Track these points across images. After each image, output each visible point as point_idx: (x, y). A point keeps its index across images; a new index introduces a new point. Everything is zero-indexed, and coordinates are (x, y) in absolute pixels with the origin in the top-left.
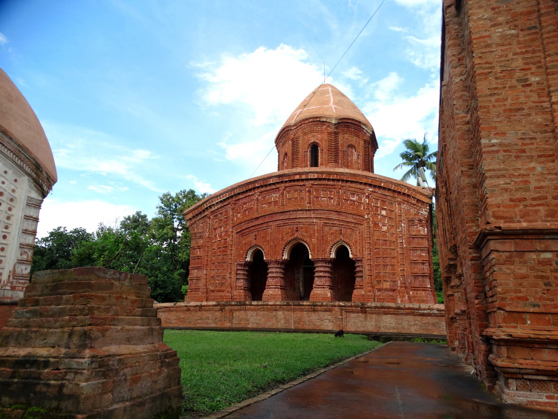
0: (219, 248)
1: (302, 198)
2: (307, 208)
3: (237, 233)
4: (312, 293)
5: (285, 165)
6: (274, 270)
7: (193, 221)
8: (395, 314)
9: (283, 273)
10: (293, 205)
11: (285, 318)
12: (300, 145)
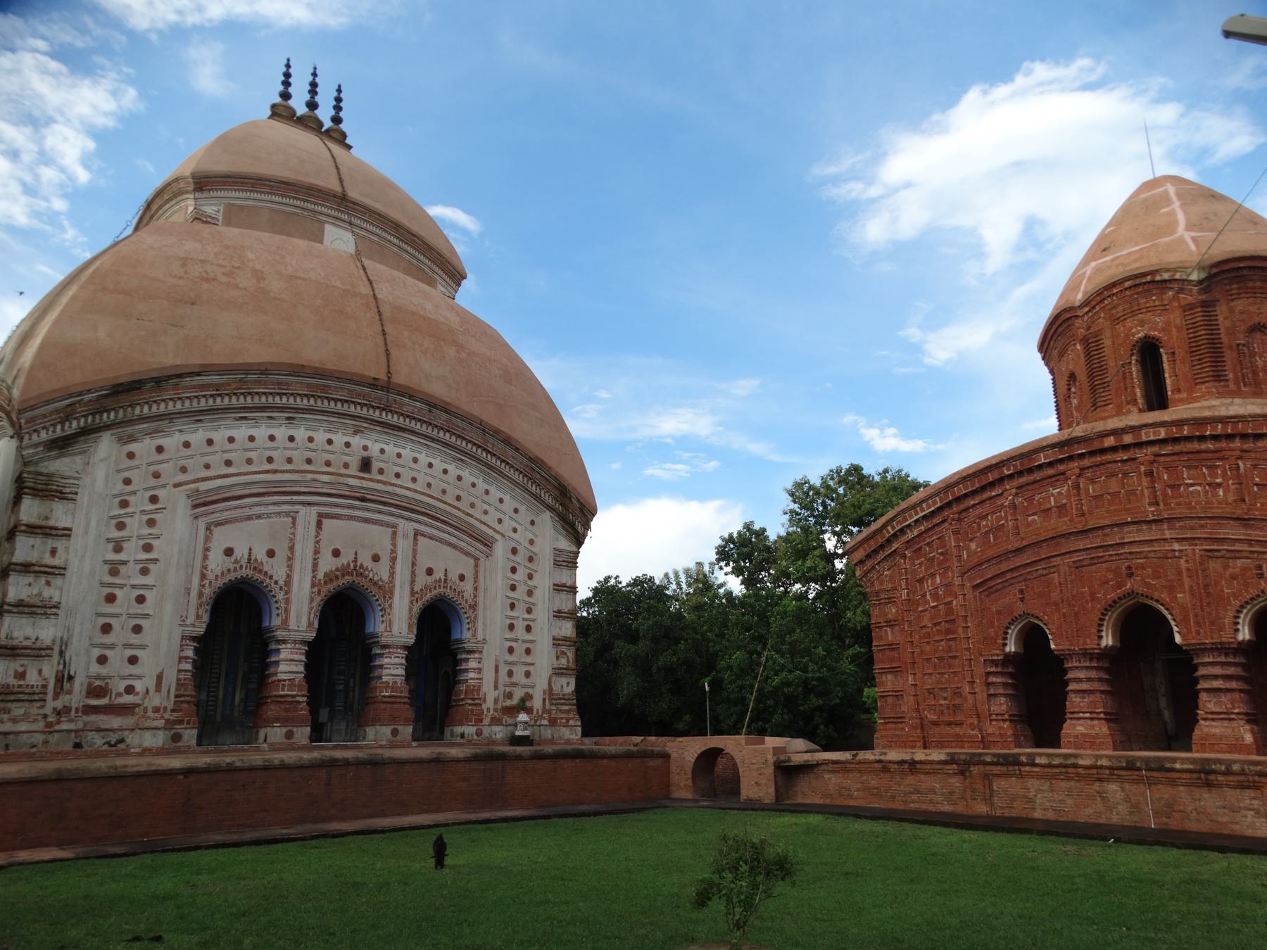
0: (935, 625)
1: (1132, 492)
2: (1151, 517)
3: (975, 587)
4: (1197, 732)
5: (1075, 402)
6: (1082, 675)
7: (868, 564)
9: (1107, 681)
10: (1108, 512)
11: (1127, 800)
12: (1107, 351)
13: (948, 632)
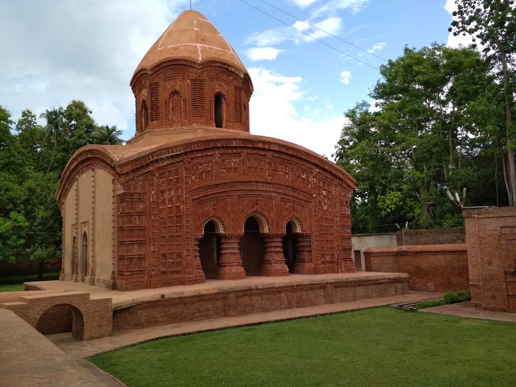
1: (261, 169)
7: (131, 176)
8: (365, 285)
11: (287, 299)
13: (177, 222)
